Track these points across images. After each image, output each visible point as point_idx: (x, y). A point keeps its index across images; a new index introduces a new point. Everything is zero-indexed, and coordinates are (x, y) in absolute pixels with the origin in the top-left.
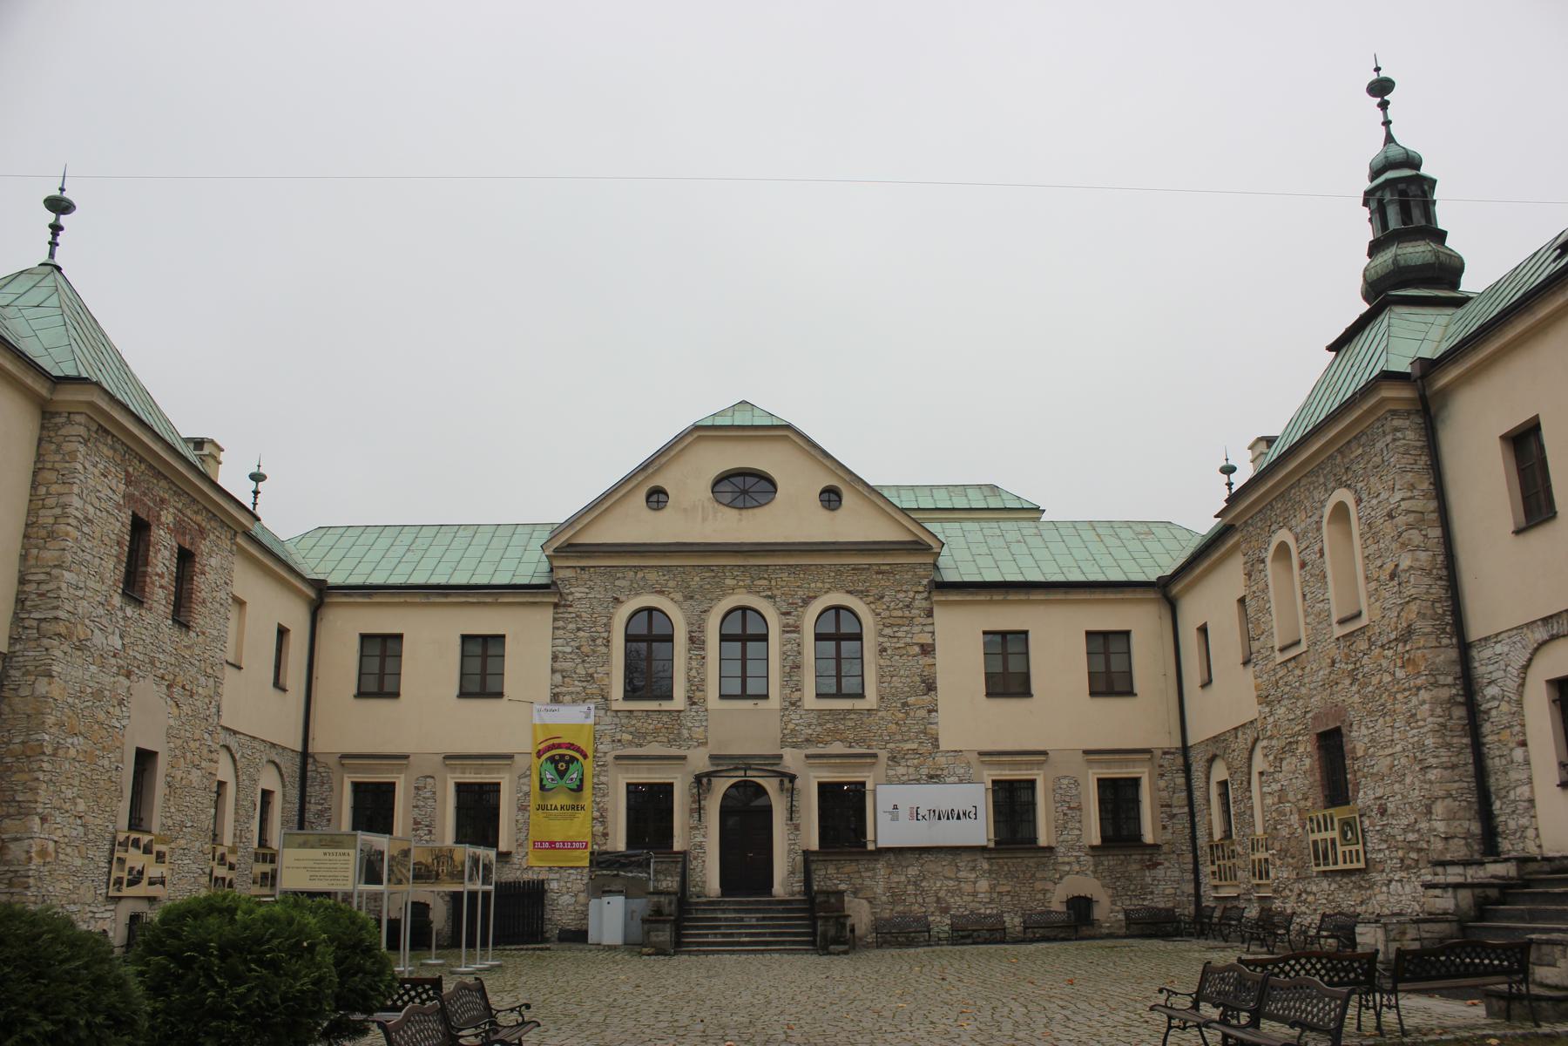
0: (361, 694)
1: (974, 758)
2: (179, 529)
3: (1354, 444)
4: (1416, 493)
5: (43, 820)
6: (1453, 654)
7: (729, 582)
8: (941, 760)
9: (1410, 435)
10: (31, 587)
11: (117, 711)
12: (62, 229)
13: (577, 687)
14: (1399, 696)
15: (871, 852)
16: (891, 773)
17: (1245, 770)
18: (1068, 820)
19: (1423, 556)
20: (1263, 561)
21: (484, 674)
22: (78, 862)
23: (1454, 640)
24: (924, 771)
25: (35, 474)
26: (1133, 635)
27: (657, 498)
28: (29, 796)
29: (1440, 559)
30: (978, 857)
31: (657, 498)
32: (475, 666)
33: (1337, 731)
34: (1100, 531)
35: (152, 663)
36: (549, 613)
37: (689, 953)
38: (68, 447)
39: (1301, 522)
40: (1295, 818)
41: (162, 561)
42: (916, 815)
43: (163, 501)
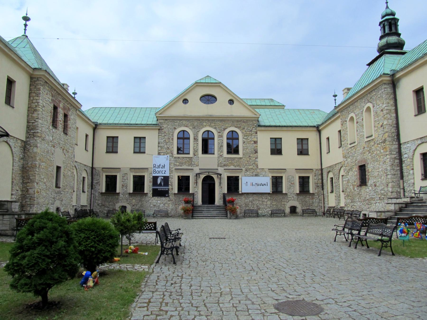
1: (267, 170)
3: (373, 91)
4: (389, 105)
5: (37, 184)
6: (397, 146)
7: (204, 124)
8: (259, 171)
9: (389, 89)
10: (31, 124)
11: (52, 156)
12: (27, 25)
13: (165, 150)
14: (381, 157)
15: (240, 194)
16: (246, 174)
17: (338, 175)
18: (291, 187)
19: (390, 121)
20: (346, 121)
22: (45, 194)
23: (397, 143)
24: (254, 173)
25: (30, 94)
26: (309, 140)
27: (185, 101)
28: (33, 178)
29: (394, 122)
30: (267, 195)
31: (185, 101)
32: (137, 145)
33: (364, 166)
34: (301, 112)
35: (59, 144)
36: (157, 131)
37: (195, 219)
39: (357, 111)
40: (351, 187)
41: (60, 117)
42: (252, 185)
43: (60, 101)
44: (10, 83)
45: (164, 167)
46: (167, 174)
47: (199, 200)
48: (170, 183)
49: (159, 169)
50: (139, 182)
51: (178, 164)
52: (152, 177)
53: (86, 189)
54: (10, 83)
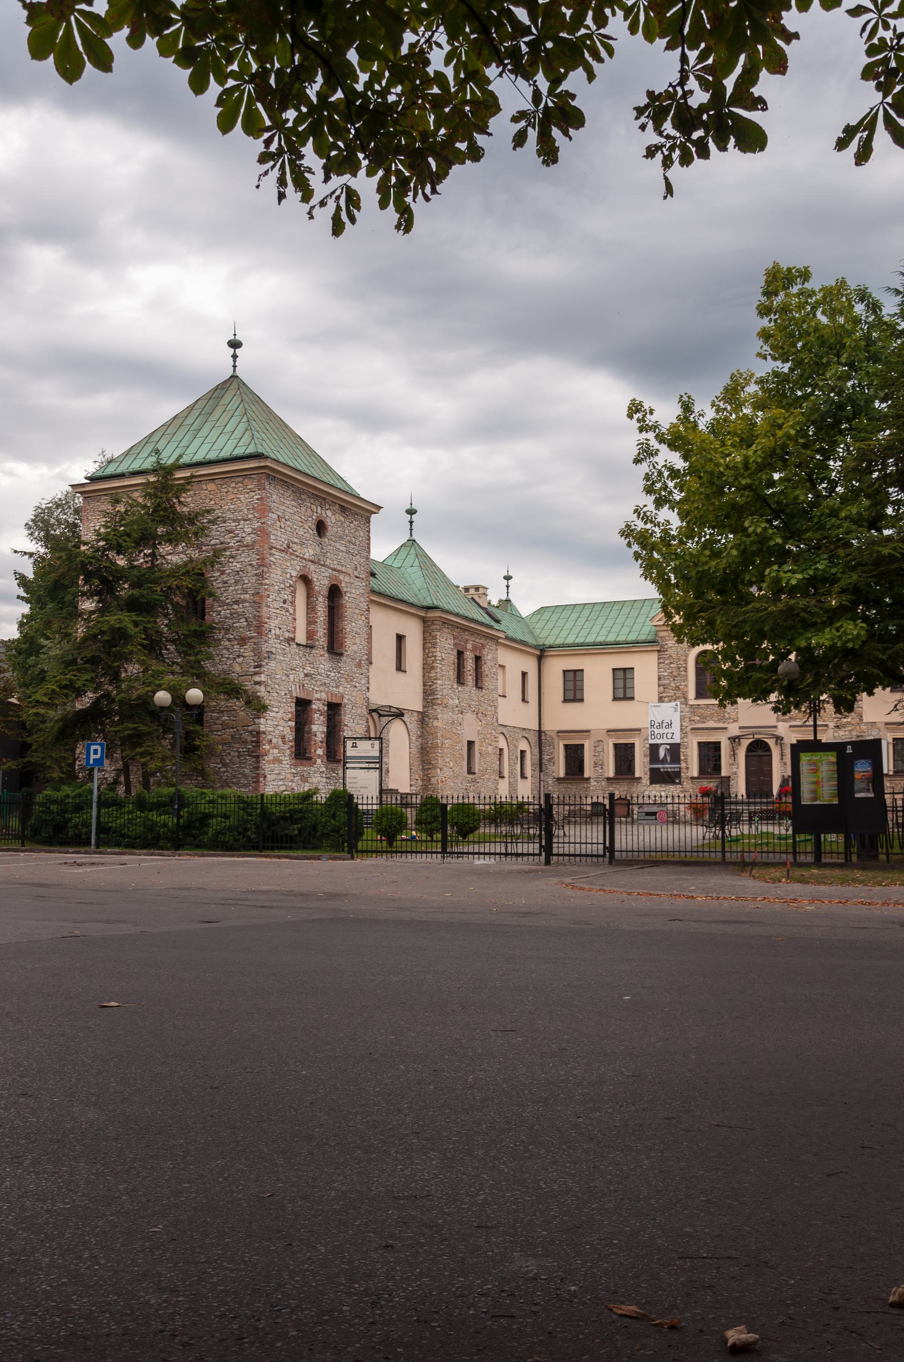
0: (566, 701)
1: (882, 726)
2: (475, 648)
8: (864, 727)
10: (427, 687)
11: (459, 728)
16: (836, 734)
21: (625, 688)
25: (424, 644)
32: (620, 683)
36: (655, 656)
38: (434, 634)
41: (469, 665)
44: (400, 638)
45: (670, 725)
46: (677, 739)
47: (739, 788)
48: (682, 758)
49: (661, 731)
50: (624, 754)
51: (697, 718)
52: (648, 746)
53: (528, 772)
54: (400, 638)
